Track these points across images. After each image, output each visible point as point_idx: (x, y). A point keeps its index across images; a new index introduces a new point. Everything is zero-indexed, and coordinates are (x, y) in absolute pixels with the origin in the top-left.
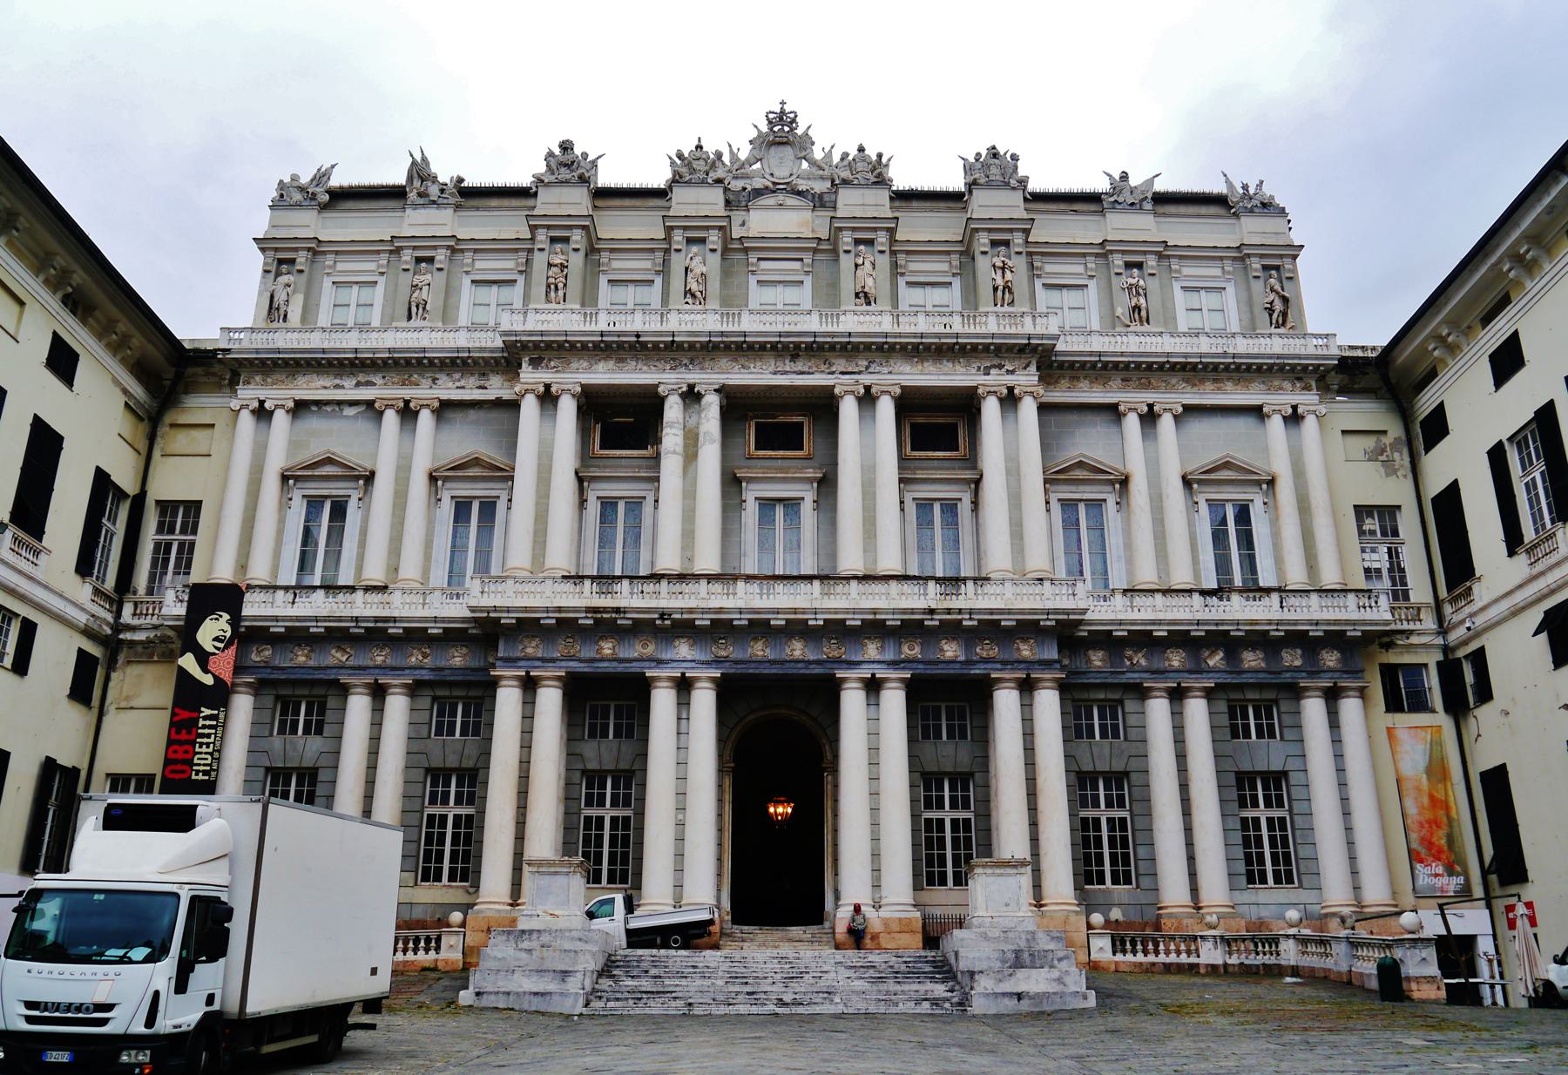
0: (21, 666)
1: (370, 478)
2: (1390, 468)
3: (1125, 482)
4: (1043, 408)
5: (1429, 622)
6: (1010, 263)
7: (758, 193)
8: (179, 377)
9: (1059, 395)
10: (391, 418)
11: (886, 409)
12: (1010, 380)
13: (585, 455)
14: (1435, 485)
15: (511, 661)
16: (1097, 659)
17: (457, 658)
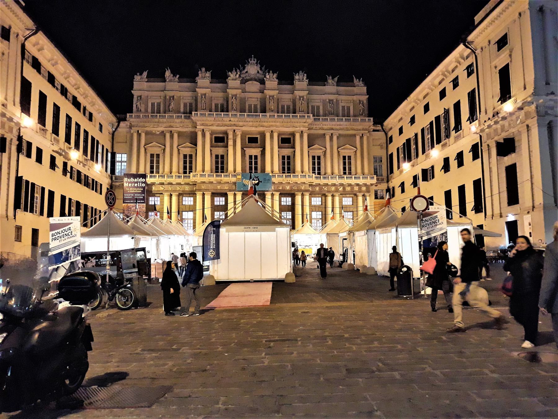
0: (101, 194)
1: (164, 150)
2: (382, 148)
3: (325, 152)
4: (309, 136)
5: (385, 180)
6: (303, 102)
7: (247, 80)
8: (118, 125)
9: (312, 132)
10: (168, 136)
11: (276, 135)
12: (302, 129)
13: (212, 146)
14: (390, 153)
15: (200, 190)
16: (317, 189)
17: (187, 188)
